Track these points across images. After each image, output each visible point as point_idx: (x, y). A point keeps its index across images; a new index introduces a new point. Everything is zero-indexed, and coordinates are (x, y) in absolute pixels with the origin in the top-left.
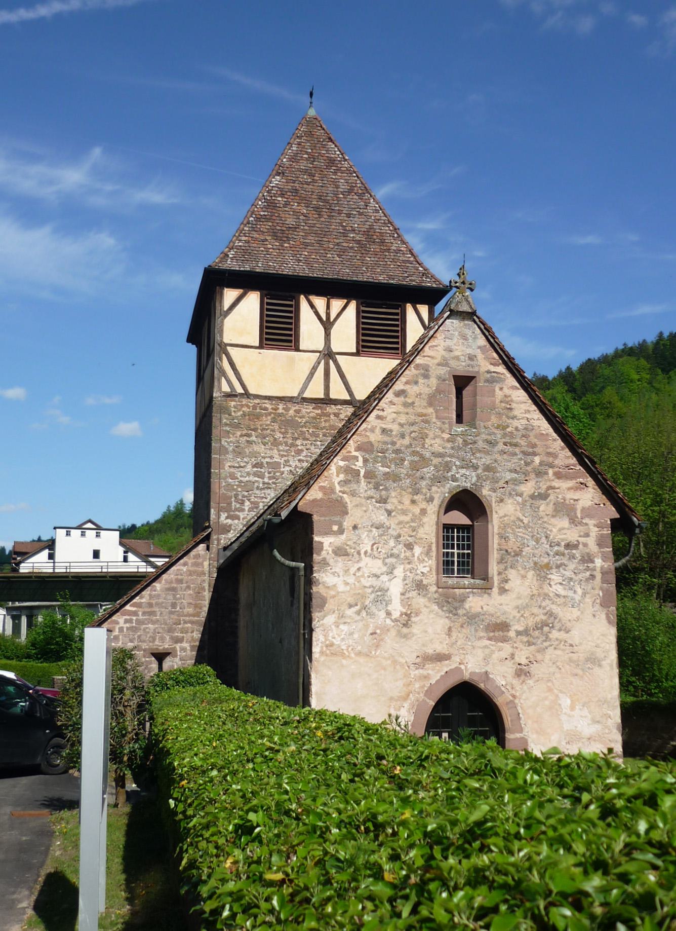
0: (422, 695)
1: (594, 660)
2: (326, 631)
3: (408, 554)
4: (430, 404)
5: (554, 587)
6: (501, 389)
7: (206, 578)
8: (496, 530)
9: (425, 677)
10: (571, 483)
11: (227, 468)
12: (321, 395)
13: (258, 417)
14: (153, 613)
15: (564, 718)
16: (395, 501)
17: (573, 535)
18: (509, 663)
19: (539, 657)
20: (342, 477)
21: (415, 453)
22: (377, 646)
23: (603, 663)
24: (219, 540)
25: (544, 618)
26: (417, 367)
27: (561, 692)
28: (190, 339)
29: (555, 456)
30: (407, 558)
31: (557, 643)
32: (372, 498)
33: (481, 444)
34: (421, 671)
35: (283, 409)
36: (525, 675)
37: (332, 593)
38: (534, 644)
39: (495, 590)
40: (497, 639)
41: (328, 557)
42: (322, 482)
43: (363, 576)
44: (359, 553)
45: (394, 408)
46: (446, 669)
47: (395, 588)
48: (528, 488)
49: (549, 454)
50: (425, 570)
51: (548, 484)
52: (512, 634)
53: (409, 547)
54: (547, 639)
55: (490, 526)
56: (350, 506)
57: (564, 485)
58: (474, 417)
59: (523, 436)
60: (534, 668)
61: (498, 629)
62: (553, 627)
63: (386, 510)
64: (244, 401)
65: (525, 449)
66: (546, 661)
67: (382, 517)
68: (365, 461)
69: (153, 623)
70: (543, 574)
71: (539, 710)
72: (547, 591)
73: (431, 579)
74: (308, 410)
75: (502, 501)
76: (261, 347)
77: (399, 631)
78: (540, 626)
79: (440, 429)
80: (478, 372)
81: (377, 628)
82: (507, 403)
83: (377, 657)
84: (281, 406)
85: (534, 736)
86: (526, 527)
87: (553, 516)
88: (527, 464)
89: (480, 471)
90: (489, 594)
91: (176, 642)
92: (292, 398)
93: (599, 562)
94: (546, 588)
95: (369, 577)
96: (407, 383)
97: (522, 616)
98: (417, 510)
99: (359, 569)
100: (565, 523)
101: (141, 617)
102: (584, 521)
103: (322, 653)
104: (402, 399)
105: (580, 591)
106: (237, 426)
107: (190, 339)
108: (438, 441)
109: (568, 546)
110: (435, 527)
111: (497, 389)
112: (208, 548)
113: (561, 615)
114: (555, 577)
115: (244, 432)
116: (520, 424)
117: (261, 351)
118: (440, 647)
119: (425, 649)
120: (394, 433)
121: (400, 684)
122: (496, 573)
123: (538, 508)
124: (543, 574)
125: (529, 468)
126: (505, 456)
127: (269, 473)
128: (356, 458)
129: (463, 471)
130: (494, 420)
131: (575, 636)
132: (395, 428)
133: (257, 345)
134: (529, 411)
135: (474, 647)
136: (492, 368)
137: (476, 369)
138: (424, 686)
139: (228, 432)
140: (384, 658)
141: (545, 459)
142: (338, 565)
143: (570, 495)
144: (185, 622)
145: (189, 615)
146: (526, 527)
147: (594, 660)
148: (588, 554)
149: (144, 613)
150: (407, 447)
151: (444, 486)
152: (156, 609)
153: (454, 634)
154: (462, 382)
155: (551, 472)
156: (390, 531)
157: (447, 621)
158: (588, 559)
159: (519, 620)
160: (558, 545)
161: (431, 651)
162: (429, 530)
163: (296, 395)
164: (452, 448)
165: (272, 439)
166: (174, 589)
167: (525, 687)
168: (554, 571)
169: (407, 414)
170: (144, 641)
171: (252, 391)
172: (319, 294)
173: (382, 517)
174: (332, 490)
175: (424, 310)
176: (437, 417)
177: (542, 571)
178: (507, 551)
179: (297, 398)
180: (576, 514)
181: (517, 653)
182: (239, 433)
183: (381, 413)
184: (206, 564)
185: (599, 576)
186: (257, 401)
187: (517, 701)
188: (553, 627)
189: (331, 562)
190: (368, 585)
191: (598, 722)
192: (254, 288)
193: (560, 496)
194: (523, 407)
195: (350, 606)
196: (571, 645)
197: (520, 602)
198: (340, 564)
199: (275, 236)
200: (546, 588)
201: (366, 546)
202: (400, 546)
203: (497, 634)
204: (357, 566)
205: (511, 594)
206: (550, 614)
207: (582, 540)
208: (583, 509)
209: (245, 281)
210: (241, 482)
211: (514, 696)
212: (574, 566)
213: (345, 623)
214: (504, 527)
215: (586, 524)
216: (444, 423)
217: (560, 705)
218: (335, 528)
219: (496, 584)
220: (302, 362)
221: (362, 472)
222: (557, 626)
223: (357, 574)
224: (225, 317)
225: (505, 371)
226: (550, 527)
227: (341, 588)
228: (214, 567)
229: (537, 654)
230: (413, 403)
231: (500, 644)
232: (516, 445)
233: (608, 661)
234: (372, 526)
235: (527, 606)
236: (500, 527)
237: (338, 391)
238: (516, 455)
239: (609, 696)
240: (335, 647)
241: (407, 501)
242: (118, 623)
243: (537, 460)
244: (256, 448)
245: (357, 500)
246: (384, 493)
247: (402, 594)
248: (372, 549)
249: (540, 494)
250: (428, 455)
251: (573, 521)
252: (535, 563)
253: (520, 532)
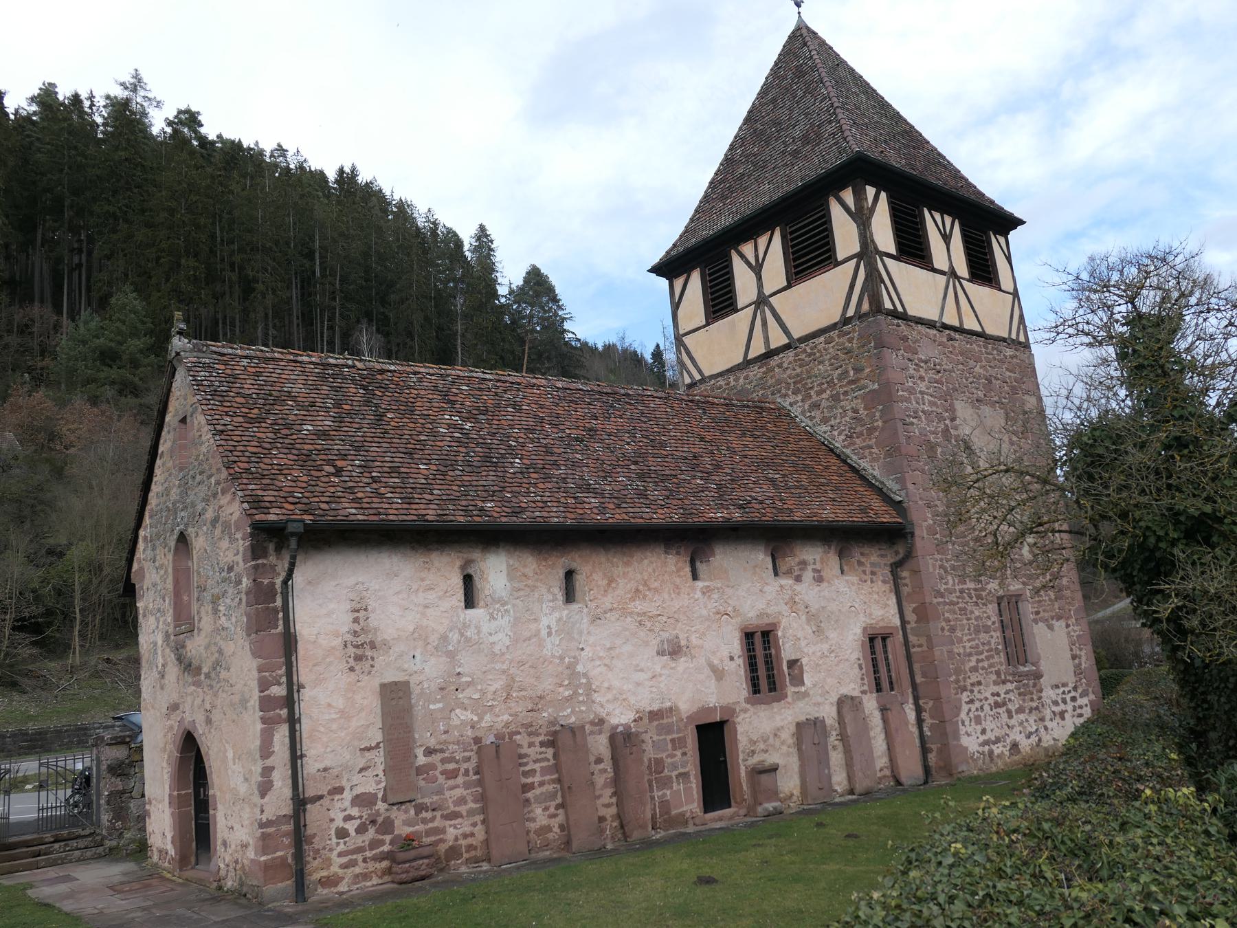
10: (228, 497)
15: (230, 772)
42: (137, 556)
52: (202, 677)
73: (171, 630)
74: (755, 372)
93: (245, 580)
105: (234, 620)
118: (175, 697)
172: (745, 240)
175: (848, 196)
192: (694, 268)
220: (741, 320)
237: (778, 339)
243: (213, 480)
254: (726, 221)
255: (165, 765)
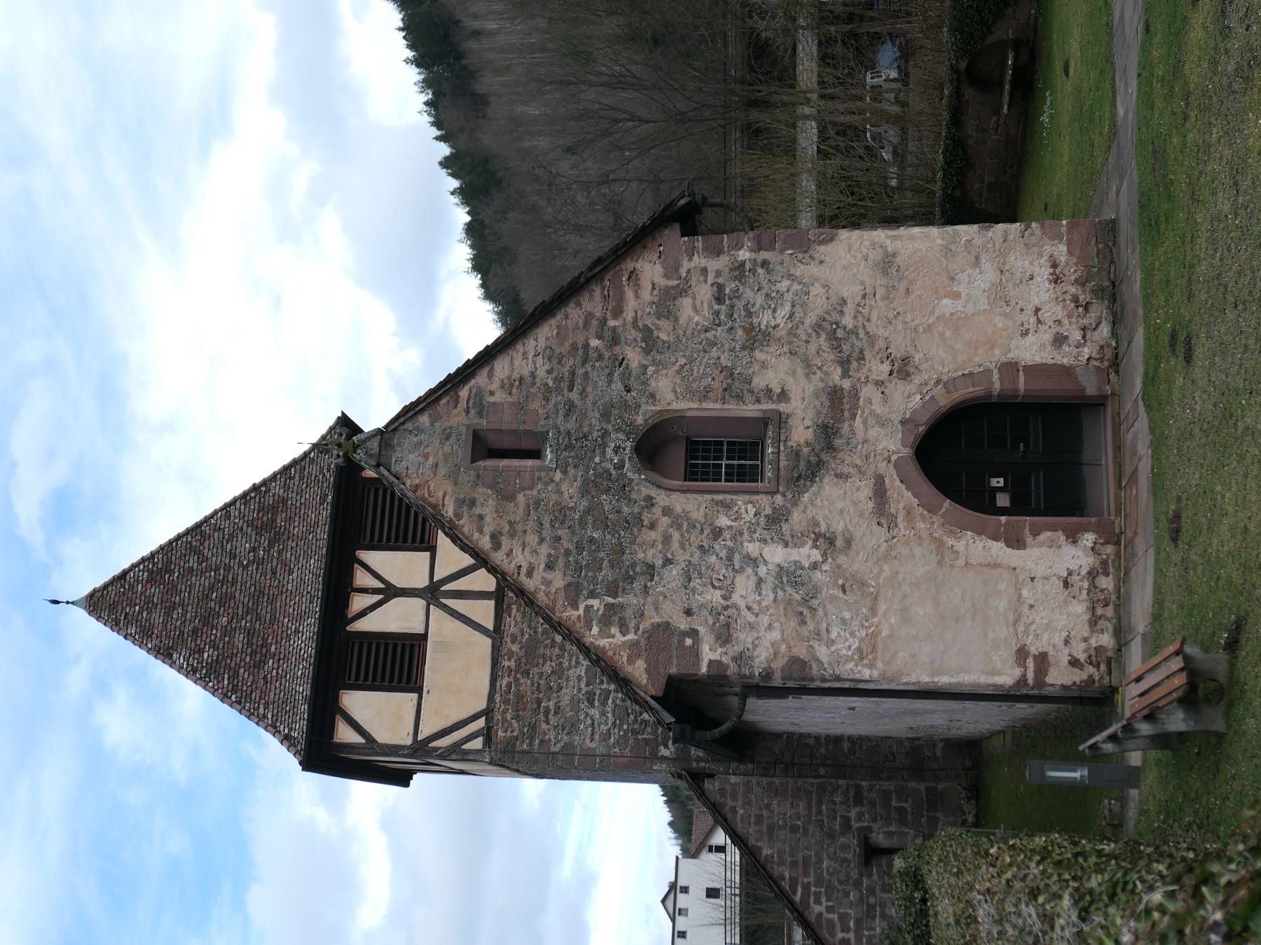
0: (935, 519)
1: (887, 263)
2: (838, 660)
3: (727, 535)
4: (512, 498)
5: (779, 321)
6: (492, 393)
7: (754, 780)
8: (695, 405)
9: (909, 513)
10: (629, 294)
11: (593, 745)
12: (493, 602)
13: (520, 697)
14: (806, 860)
15: (970, 309)
16: (650, 553)
17: (704, 292)
18: (890, 387)
19: (881, 344)
20: (614, 630)
21: (582, 523)
22: (863, 584)
23: (890, 249)
24: (699, 760)
25: (823, 336)
26: (458, 516)
27: (932, 312)
28: (407, 785)
29: (589, 316)
30: (734, 538)
31: (860, 318)
32: (645, 586)
33: (571, 425)
34: (900, 519)
35: (509, 660)
36: (906, 365)
37: (783, 648)
38: (861, 352)
39: (782, 407)
40: (855, 407)
41: (731, 654)
43: (759, 603)
44: (726, 608)
45: (517, 551)
46: (898, 482)
47: (776, 555)
48: (634, 357)
49: (586, 325)
50: (752, 510)
51: (629, 326)
52: (846, 384)
53: (717, 533)
54: (854, 332)
55: (690, 414)
56: (657, 620)
57: (631, 303)
58: (533, 434)
59: (560, 363)
60: (897, 351)
61: (838, 404)
62: (837, 324)
63: (664, 566)
64: (498, 716)
65: (579, 360)
66: (886, 334)
67: (674, 572)
68: (592, 595)
69: (820, 861)
70: (760, 337)
71: (958, 346)
72: (784, 332)
73: (764, 500)
75: (652, 396)
76: (419, 690)
77: (841, 551)
78: (836, 342)
79: (547, 484)
80: (468, 427)
81: (835, 584)
82: (512, 385)
83: (878, 584)
84: (506, 664)
85: (997, 352)
86: (691, 360)
87: (676, 320)
88: (600, 357)
89: (610, 427)
90: (788, 416)
91: (850, 827)
92: (493, 647)
93: (744, 255)
94: (781, 332)
95: (760, 594)
96: (481, 531)
97: (820, 368)
98: (665, 521)
99: (749, 608)
100: (686, 302)
101: (811, 879)
102: (684, 275)
103: (871, 666)
104: (505, 540)
105: (786, 283)
106: (534, 727)
107: (407, 785)
108: (564, 487)
109: (719, 299)
110: (689, 495)
111: (492, 399)
112: (711, 776)
113: (819, 311)
114: (765, 319)
115: (543, 718)
116: (542, 368)
117: (425, 689)
118: (863, 491)
119: (867, 513)
120: (553, 552)
121: (918, 551)
122: (757, 407)
123: (664, 342)
124: (760, 337)
125: (607, 355)
126: (589, 389)
127: (602, 682)
128: (588, 608)
129: (609, 451)
130: (536, 405)
131: (850, 291)
132: (544, 550)
133: (415, 696)
134: (525, 354)
135: (866, 441)
136: (463, 404)
137: (463, 429)
138: (921, 515)
139: (542, 741)
140: (880, 573)
141: (593, 331)
142: (744, 638)
143: (646, 295)
144: (820, 812)
145: (809, 807)
146: (691, 360)
147: (887, 263)
148: (731, 270)
149: (806, 874)
150: (573, 533)
151: (631, 480)
152: (800, 856)
153: (846, 470)
154: (484, 447)
155: (612, 323)
156: (695, 560)
157: (827, 479)
158: (739, 270)
159: (827, 374)
160: (717, 313)
161: (871, 505)
162: (693, 504)
163: (489, 641)
164: (576, 467)
165: (553, 678)
166: (771, 828)
167: (925, 366)
168: (755, 320)
169: (525, 532)
170: (848, 875)
171: (482, 704)
172: (346, 603)
173: (674, 572)
174: (635, 644)
176: (531, 488)
177: (756, 338)
178: (725, 390)
179: (494, 639)
180: (673, 287)
181: (873, 377)
182: (544, 726)
183: (524, 570)
184: (733, 779)
185: (764, 255)
186: (498, 698)
187: (945, 378)
188: (837, 324)
189: (738, 649)
190: (772, 596)
191: (977, 258)
192: (336, 699)
193: (648, 310)
194: (518, 361)
195: (804, 623)
196: (864, 296)
197: (799, 371)
198: (742, 636)
199: (259, 665)
200: (781, 332)
201: (715, 596)
202: (717, 547)
203: (847, 407)
204: (745, 612)
205: (789, 385)
206: (818, 327)
207: (711, 279)
208: (667, 276)
209: (324, 711)
210: (614, 724)
211: (938, 382)
212: (748, 290)
213: (828, 631)
214: (691, 393)
215: (689, 271)
216: (540, 479)
217: (952, 314)
218: (689, 642)
219: (773, 406)
220: (442, 628)
221: (610, 600)
222: (835, 316)
223: (756, 611)
224: (374, 741)
225: (467, 388)
226: (692, 325)
227: (776, 635)
228: (738, 768)
229: (877, 348)
230: (510, 522)
231: (861, 403)
232: (573, 373)
233: (888, 242)
234: (686, 588)
235: (807, 363)
236: (691, 400)
238: (586, 372)
239: (939, 241)
240: (864, 647)
241: (653, 535)
242: (820, 914)
243: (594, 343)
244: (565, 701)
245: (649, 611)
246: (638, 569)
247: (786, 545)
248: (720, 588)
249: (644, 340)
250: (585, 503)
251: (682, 291)
252: (743, 348)
253: (698, 370)
254: (302, 641)
255: (960, 546)
